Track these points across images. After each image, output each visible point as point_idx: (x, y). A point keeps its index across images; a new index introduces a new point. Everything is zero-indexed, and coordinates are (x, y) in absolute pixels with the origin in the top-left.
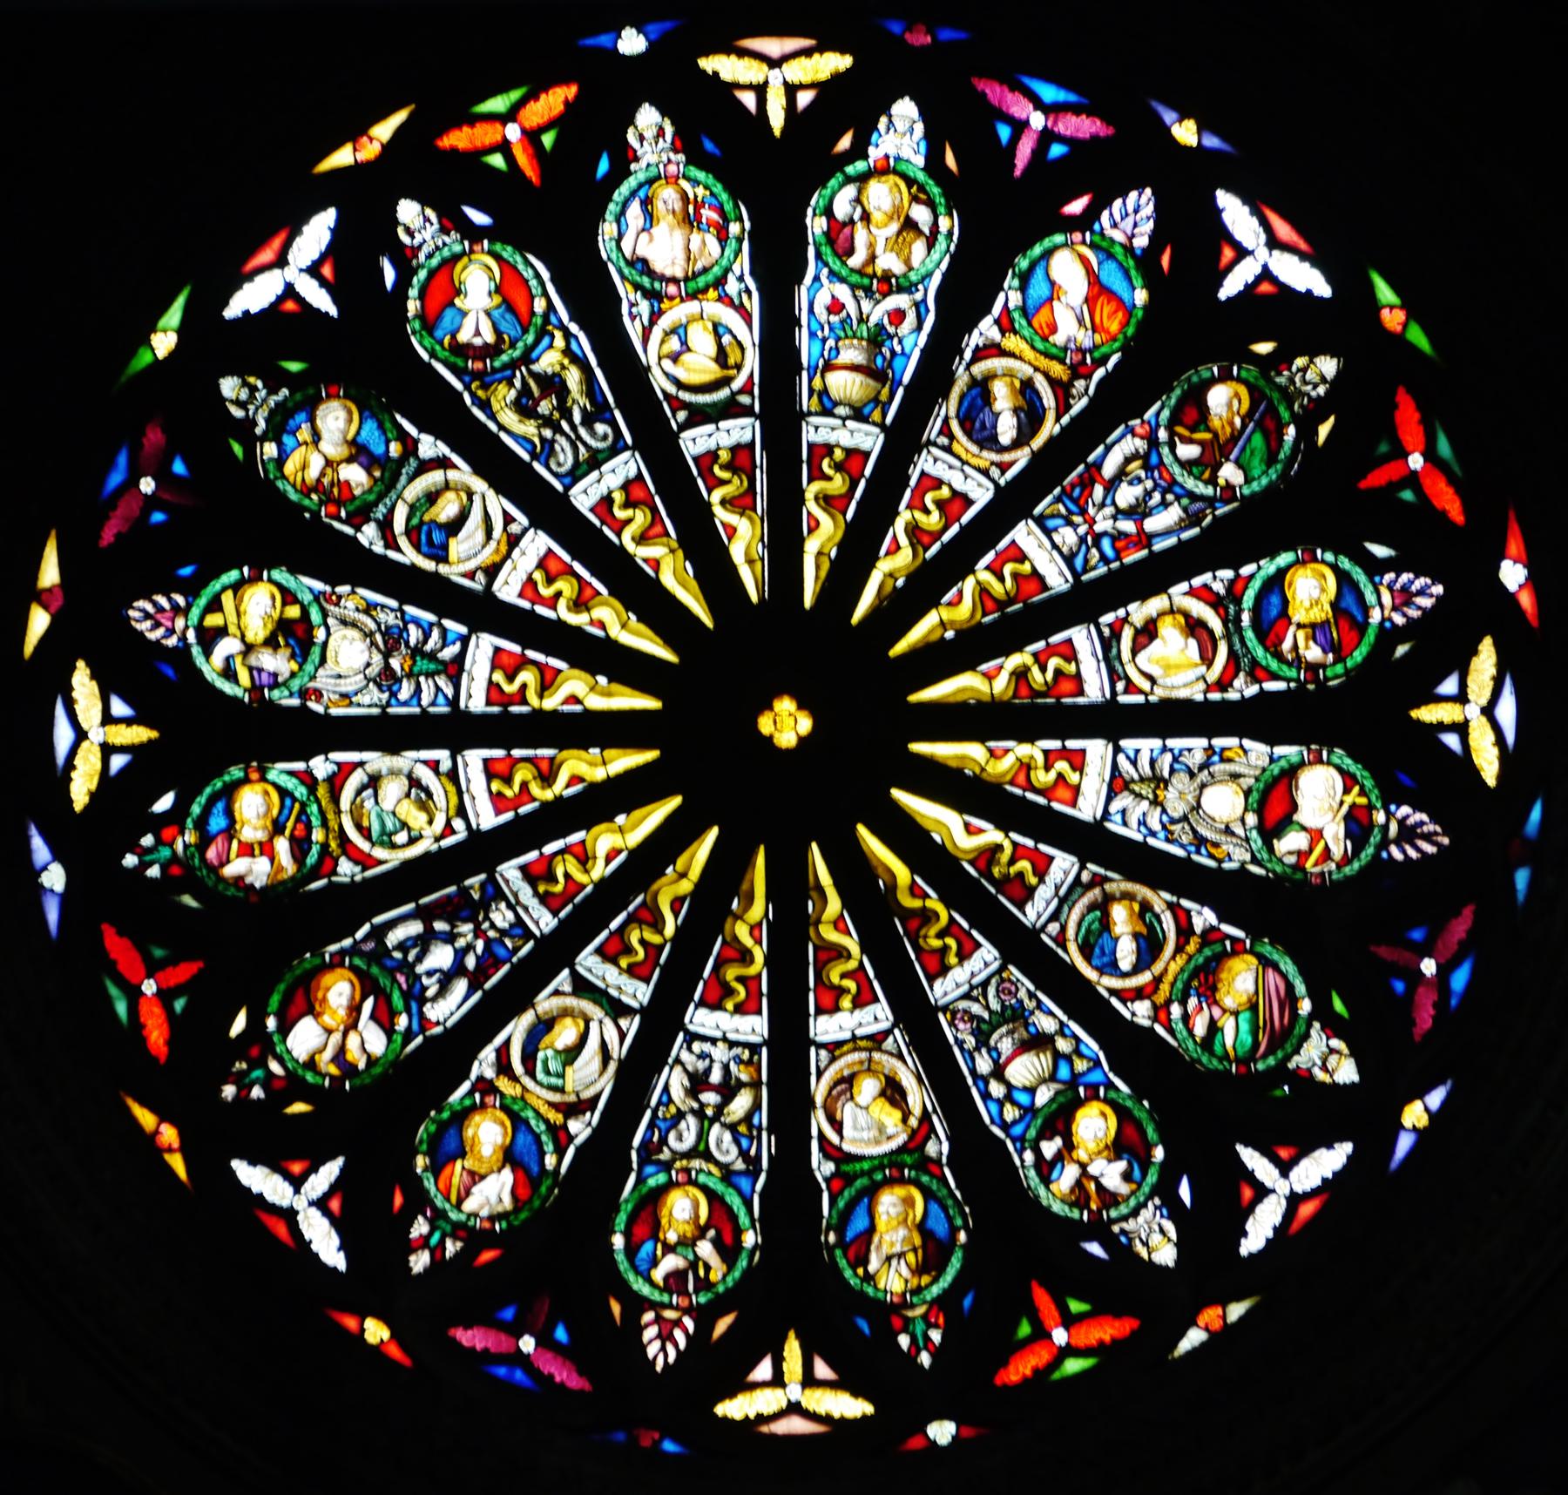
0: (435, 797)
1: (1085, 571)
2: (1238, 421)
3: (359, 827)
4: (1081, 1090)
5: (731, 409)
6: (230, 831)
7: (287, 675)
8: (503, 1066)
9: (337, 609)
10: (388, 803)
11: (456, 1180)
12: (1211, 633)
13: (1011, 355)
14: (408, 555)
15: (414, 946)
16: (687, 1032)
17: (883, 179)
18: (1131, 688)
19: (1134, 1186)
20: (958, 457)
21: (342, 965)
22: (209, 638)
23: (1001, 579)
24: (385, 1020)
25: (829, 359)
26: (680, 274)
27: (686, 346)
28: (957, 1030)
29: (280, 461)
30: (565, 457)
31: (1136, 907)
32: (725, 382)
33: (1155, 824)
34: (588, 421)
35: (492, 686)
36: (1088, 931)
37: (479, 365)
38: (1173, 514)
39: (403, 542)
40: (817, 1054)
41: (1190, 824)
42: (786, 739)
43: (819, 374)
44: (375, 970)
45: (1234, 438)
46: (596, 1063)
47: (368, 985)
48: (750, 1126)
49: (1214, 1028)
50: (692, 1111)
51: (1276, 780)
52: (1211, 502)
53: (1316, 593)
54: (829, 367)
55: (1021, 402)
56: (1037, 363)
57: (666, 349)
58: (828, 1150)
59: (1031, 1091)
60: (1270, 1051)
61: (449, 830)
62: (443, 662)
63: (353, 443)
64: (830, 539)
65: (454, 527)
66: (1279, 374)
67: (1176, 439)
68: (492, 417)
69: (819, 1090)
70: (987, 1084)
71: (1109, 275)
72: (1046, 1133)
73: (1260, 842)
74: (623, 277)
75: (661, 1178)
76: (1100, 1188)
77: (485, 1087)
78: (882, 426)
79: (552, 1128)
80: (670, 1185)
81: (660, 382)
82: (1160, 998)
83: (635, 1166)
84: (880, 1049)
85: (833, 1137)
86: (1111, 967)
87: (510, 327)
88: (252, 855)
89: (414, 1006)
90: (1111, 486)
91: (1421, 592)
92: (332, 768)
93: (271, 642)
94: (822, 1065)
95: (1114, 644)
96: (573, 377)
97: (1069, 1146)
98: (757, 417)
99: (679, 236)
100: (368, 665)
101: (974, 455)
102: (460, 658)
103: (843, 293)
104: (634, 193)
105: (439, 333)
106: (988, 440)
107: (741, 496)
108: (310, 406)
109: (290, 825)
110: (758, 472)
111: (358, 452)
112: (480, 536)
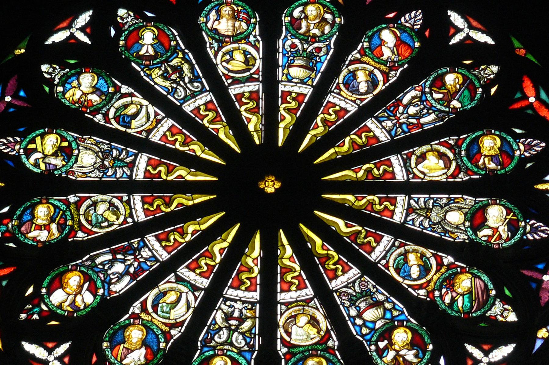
0: (120, 210)
1: (396, 136)
2: (458, 86)
3: (87, 220)
4: (396, 323)
5: (250, 79)
6: (31, 221)
7: (61, 166)
8: (144, 309)
9: (83, 144)
10: (100, 212)
11: (120, 352)
12: (448, 157)
13: (365, 63)
14: (115, 125)
15: (108, 264)
16: (224, 297)
17: (313, 5)
18: (415, 176)
19: (420, 360)
20: (343, 97)
21: (76, 270)
22: (29, 153)
23: (361, 138)
24: (93, 291)
25: (290, 63)
26: (230, 34)
27: (232, 58)
28: (342, 299)
29: (64, 93)
30: (181, 93)
31: (419, 255)
32: (249, 70)
33: (426, 224)
34: (191, 81)
35: (146, 171)
36: (398, 263)
37: (148, 63)
38: (432, 117)
39: (113, 121)
40: (281, 307)
41: (441, 225)
42: (270, 190)
43: (286, 69)
44: (90, 272)
45: (456, 92)
46: (184, 308)
47: (87, 278)
48: (251, 334)
49: (453, 300)
50: (226, 327)
51: (478, 210)
52: (448, 113)
53: (492, 145)
54: (290, 66)
55: (369, 79)
56: (375, 66)
57: (224, 59)
58: (285, 343)
59: (374, 322)
60: (478, 309)
61: (125, 221)
62: (126, 163)
63: (94, 87)
64: (289, 123)
65: (134, 116)
66: (475, 71)
67: (433, 92)
68: (152, 80)
69: (281, 321)
70: (355, 320)
71: (404, 37)
72: (381, 338)
73: (471, 232)
74: (208, 35)
75: (211, 353)
76: (405, 360)
77: (135, 316)
78: (312, 86)
79: (163, 332)
80: (215, 355)
81: (221, 70)
82: (430, 288)
83: (199, 348)
84: (308, 306)
85: (288, 339)
86: (408, 276)
87: (160, 49)
88: (41, 230)
89: (106, 285)
90: (406, 107)
91: (535, 145)
92: (76, 199)
93: (55, 154)
94: (283, 311)
95: (408, 161)
96: (186, 67)
97: (391, 343)
98: (261, 82)
99: (230, 23)
100: (95, 163)
101: (350, 96)
102: (134, 161)
103: (296, 41)
104: (213, 8)
105: (131, 52)
106: (356, 91)
107: (254, 108)
108: (78, 75)
109: (57, 219)
110: (261, 100)
111: (96, 90)
112: (145, 119)
